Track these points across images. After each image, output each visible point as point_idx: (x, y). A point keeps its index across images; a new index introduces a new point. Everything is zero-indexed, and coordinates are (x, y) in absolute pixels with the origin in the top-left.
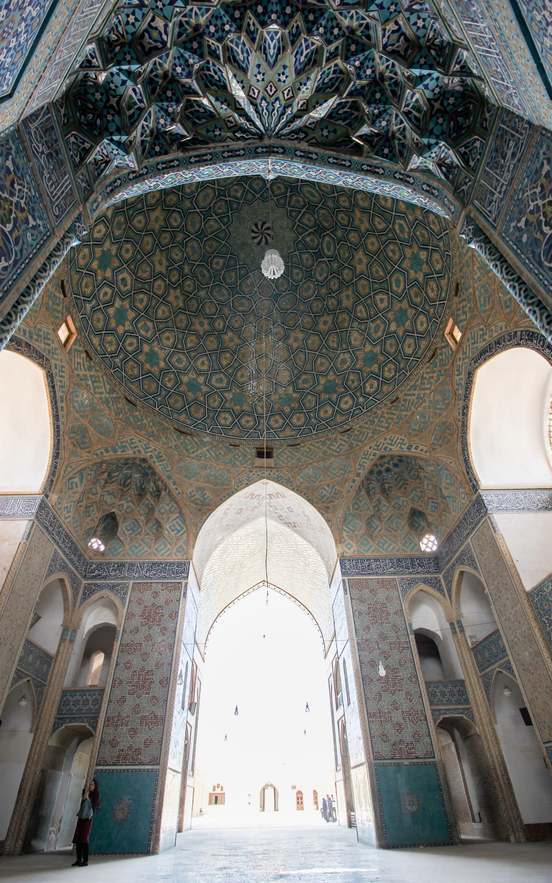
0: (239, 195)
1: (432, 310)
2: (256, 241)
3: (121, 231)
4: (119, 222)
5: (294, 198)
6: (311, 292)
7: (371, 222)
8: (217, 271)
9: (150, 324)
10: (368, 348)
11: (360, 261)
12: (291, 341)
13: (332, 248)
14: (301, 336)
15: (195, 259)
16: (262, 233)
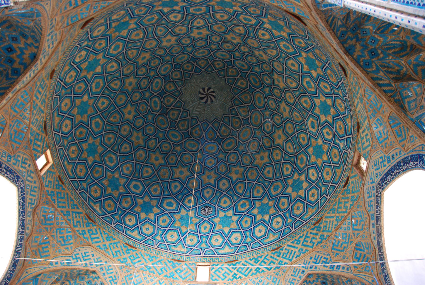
0: (223, 128)
1: (66, 143)
2: (212, 90)
3: (302, 155)
4: (302, 163)
5: (186, 127)
6: (163, 68)
7: (131, 144)
8: (243, 79)
9: (305, 84)
10: (99, 69)
11: (129, 113)
12: (174, 38)
13: (153, 104)
14: (165, 44)
15: (259, 94)
16: (207, 94)
